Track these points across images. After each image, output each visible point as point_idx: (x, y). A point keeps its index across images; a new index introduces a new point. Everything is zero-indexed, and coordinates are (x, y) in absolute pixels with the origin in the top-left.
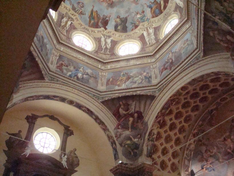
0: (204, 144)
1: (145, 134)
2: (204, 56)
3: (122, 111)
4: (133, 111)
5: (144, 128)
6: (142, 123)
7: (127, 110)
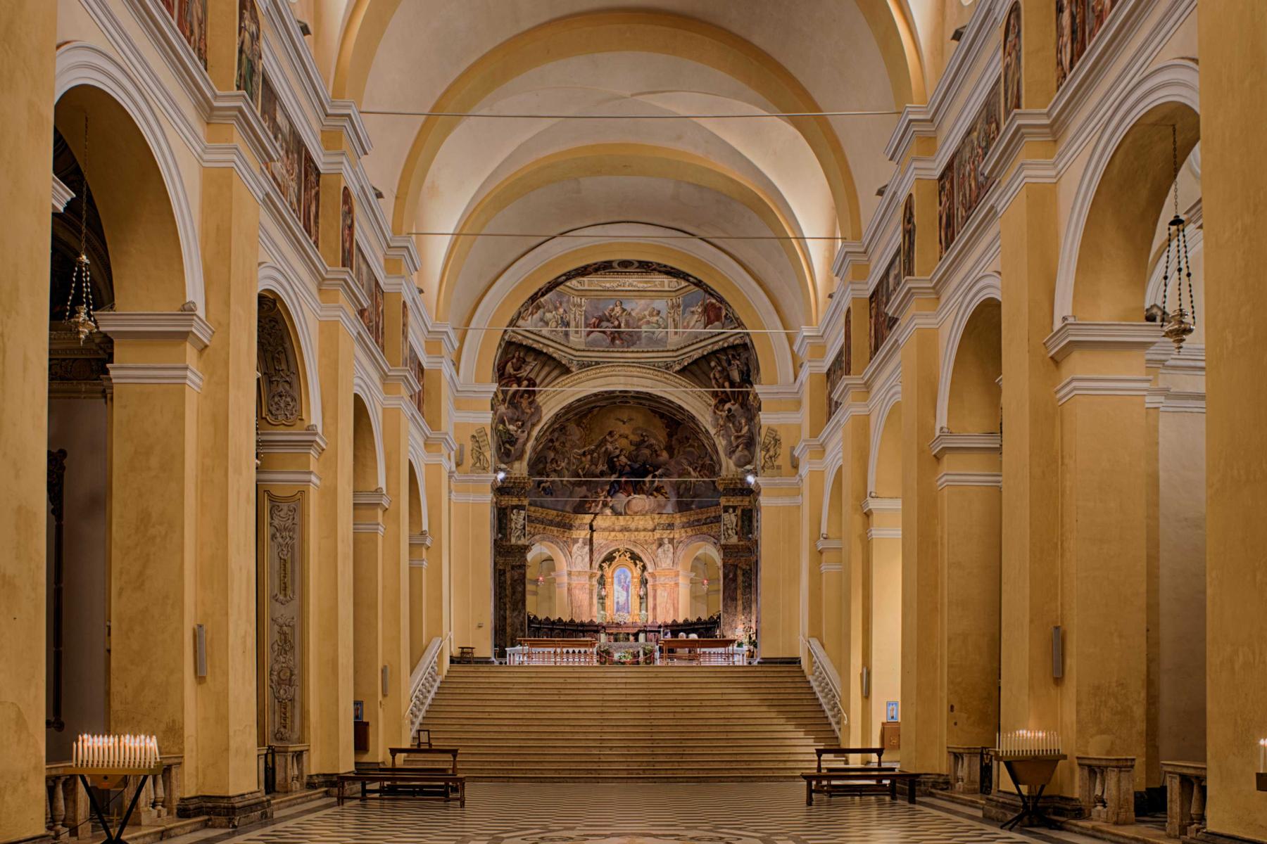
0: (555, 449)
1: (534, 425)
2: (678, 372)
3: (509, 369)
4: (525, 374)
5: (532, 414)
6: (531, 403)
7: (518, 369)
